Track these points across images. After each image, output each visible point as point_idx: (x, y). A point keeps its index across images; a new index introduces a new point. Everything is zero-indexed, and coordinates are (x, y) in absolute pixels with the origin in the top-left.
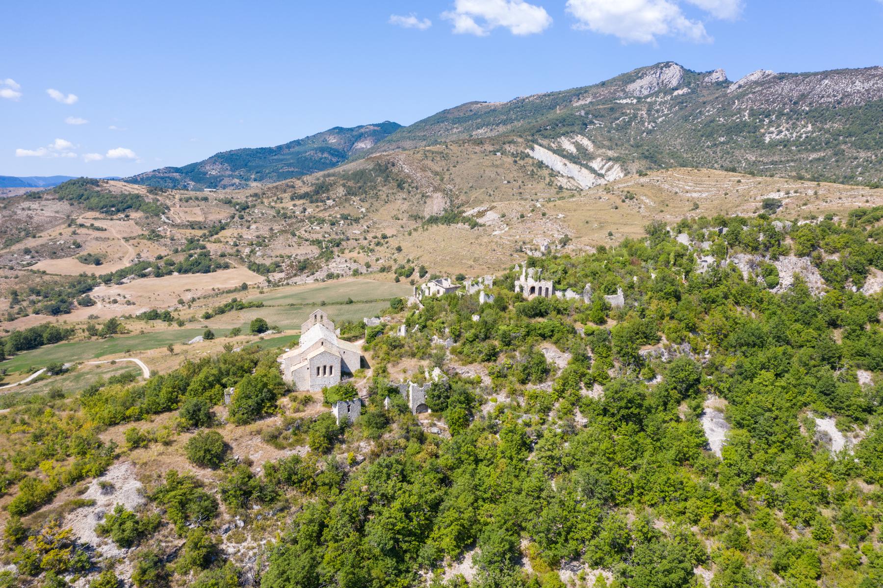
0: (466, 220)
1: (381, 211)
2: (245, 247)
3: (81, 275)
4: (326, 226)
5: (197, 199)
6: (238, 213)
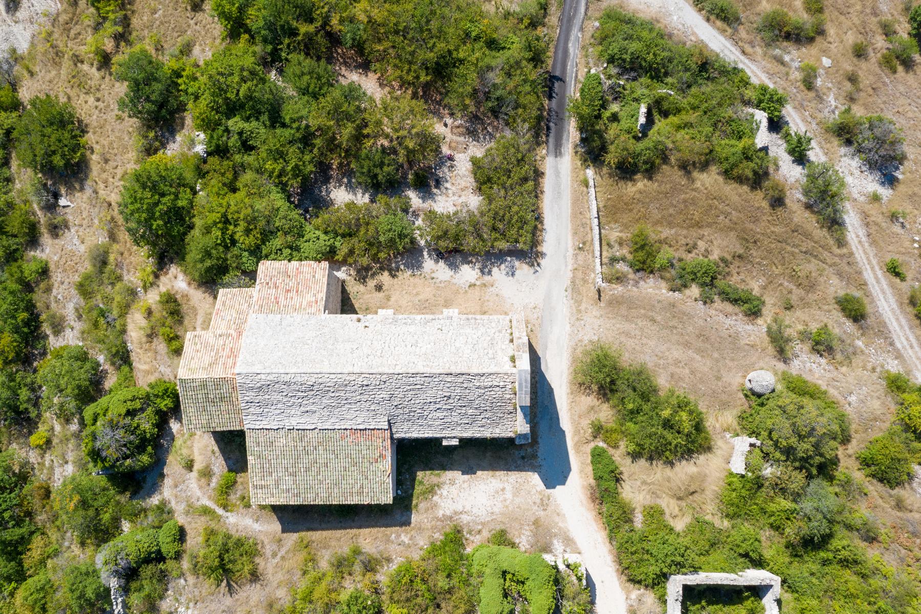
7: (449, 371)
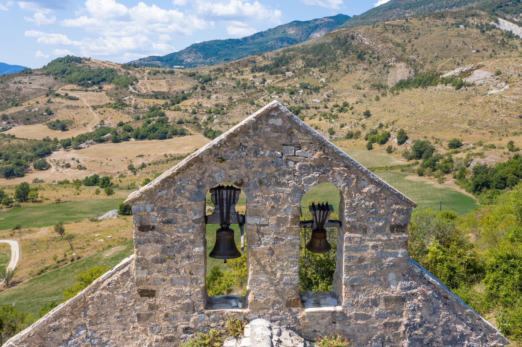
0: (446, 82)
1: (341, 81)
2: (203, 115)
3: (45, 140)
4: (286, 96)
5: (164, 72)
6: (200, 85)
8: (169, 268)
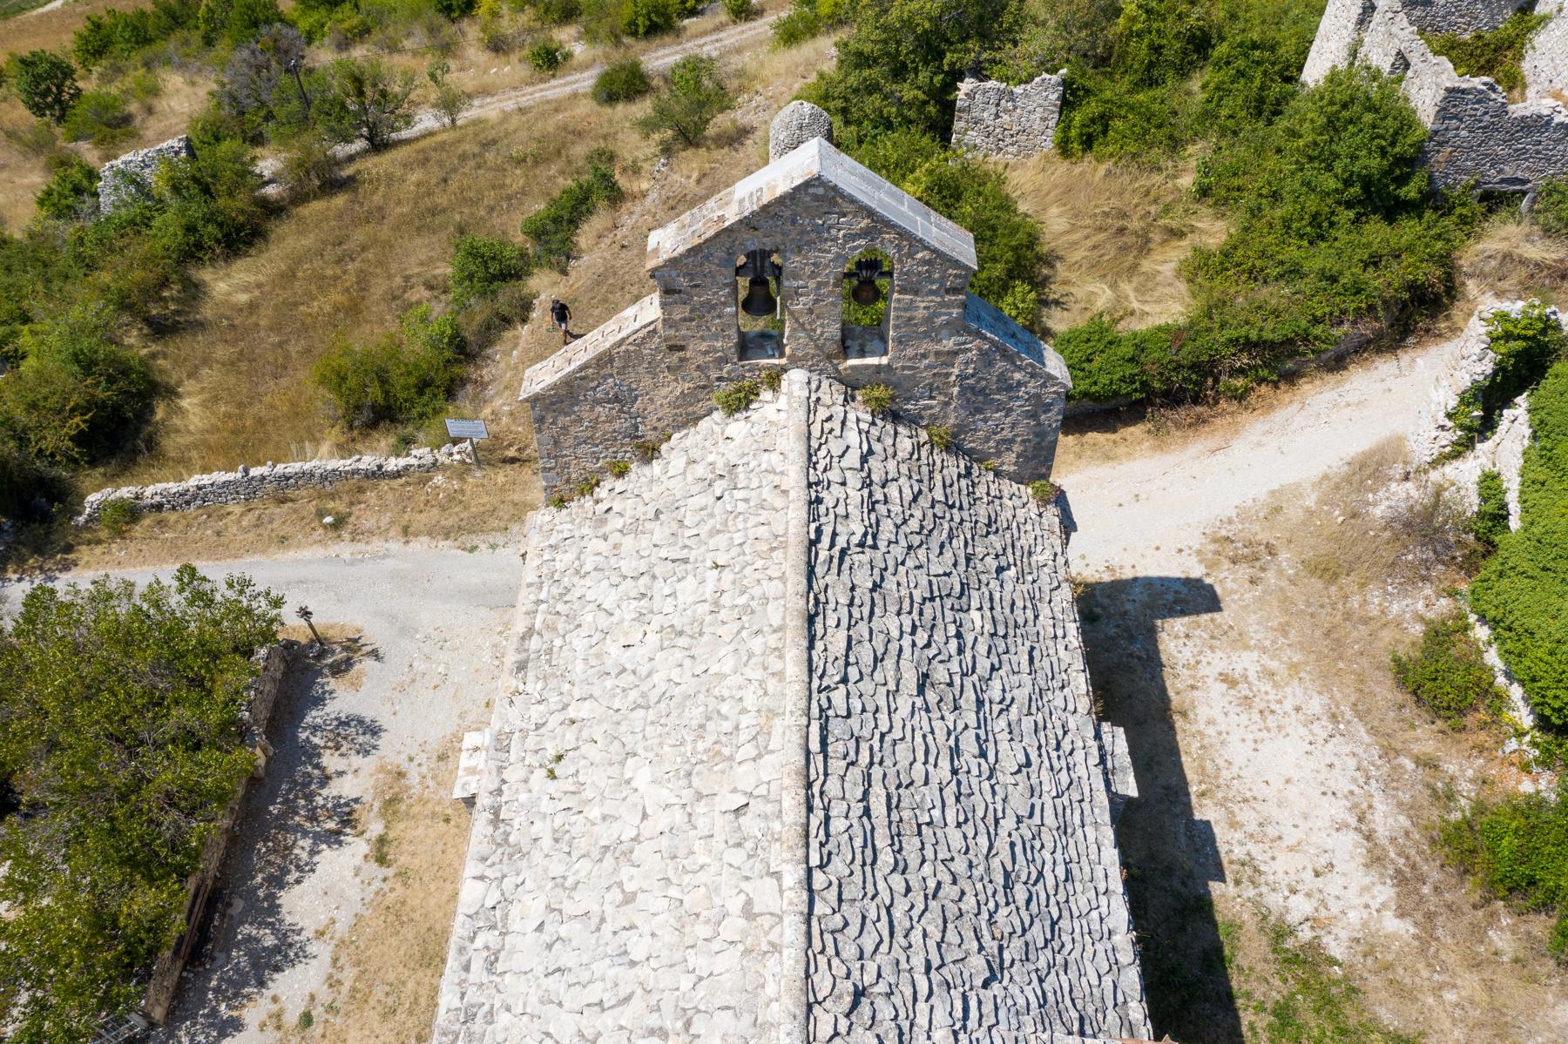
7: (796, 624)
8: (699, 326)
